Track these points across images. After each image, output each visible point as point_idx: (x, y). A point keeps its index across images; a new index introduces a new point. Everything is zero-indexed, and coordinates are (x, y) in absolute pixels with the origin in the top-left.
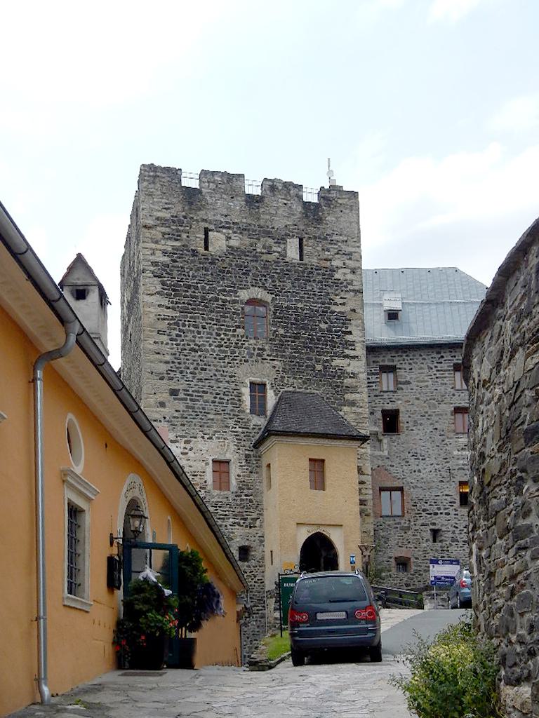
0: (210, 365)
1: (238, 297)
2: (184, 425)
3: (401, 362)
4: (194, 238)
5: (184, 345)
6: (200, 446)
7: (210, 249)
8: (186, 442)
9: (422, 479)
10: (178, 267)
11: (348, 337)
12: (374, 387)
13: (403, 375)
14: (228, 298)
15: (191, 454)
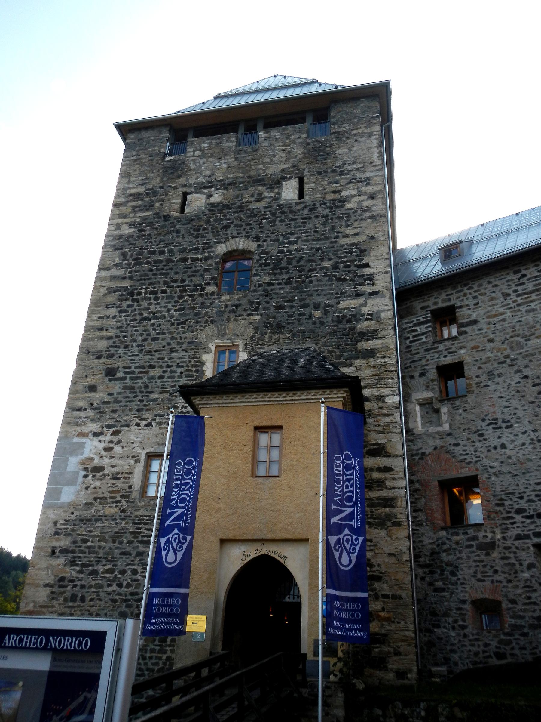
0: (164, 334)
1: (213, 252)
2: (114, 411)
3: (461, 299)
4: (168, 205)
5: (135, 315)
6: (132, 437)
7: (187, 211)
8: (113, 434)
9: (509, 457)
10: (145, 235)
11: (366, 271)
12: (424, 340)
13: (464, 314)
14: (200, 256)
15: (118, 449)
